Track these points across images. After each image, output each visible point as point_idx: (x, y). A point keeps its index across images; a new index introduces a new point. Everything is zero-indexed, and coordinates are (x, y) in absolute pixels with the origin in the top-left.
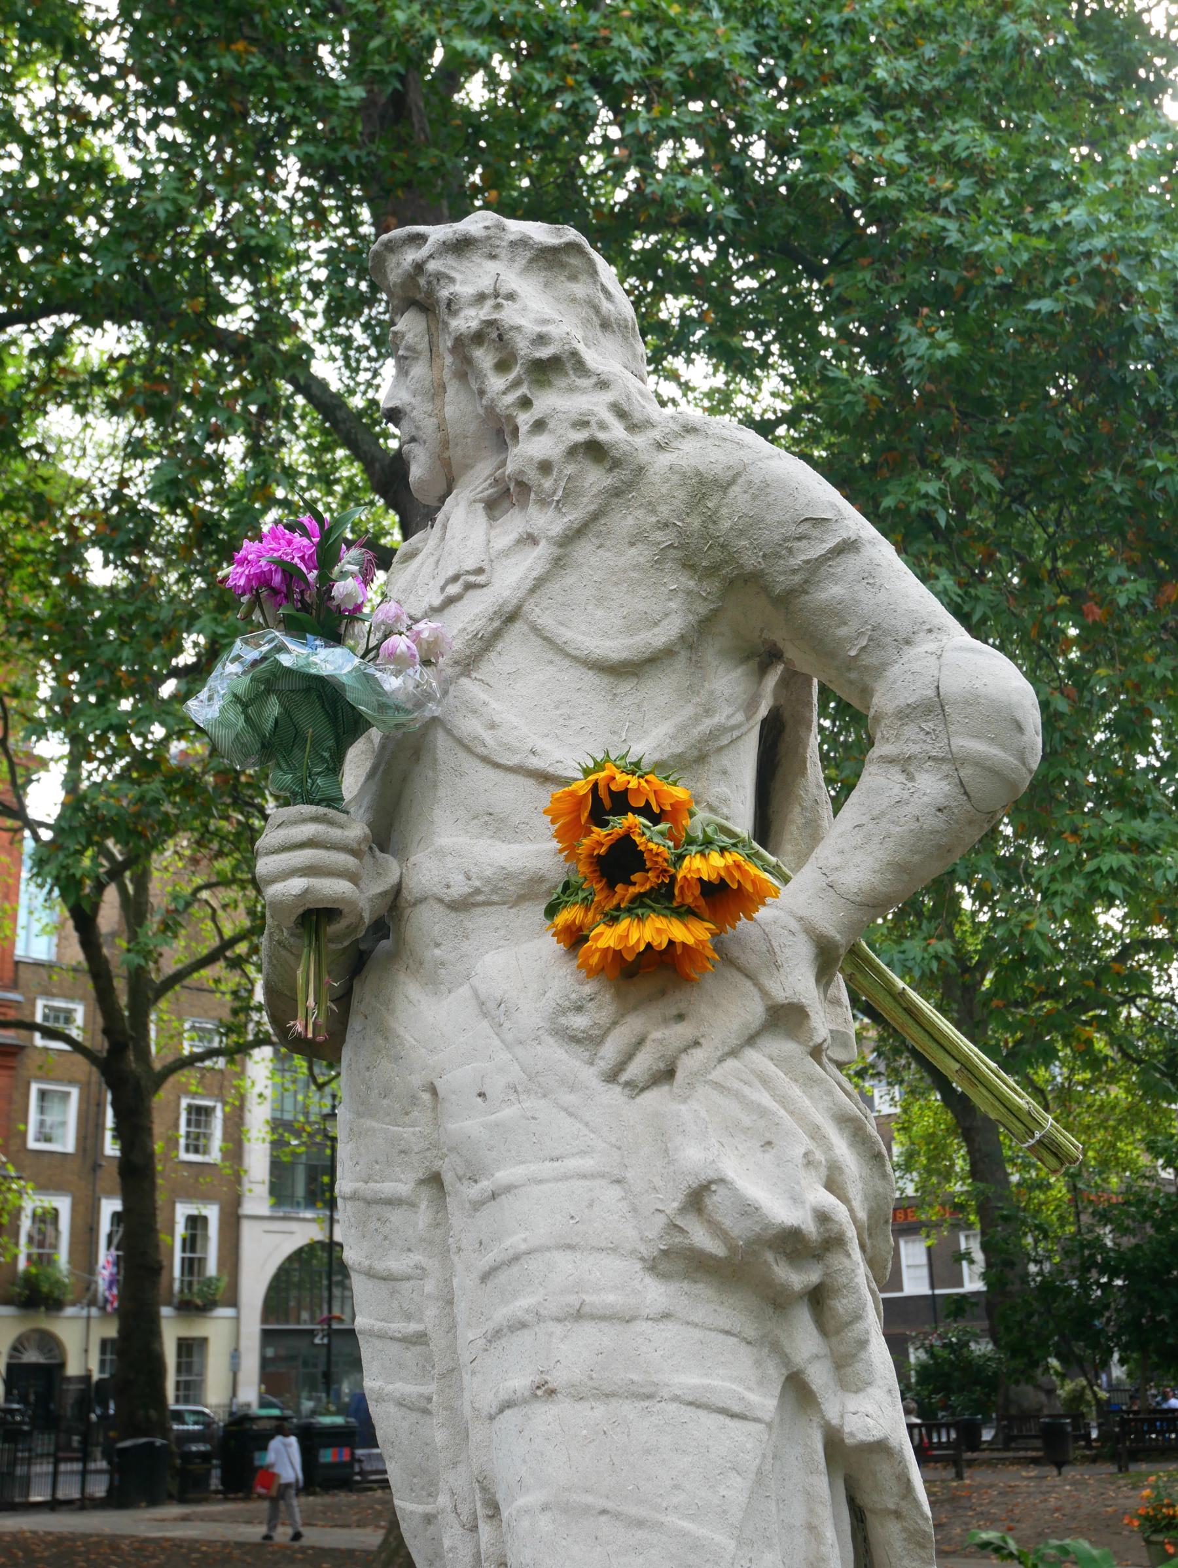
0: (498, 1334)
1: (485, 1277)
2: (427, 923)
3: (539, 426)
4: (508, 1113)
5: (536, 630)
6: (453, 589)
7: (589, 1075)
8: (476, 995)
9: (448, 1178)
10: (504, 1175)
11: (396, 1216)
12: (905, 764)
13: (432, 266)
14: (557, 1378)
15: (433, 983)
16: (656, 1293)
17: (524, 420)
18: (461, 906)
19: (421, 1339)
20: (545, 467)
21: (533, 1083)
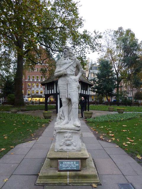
2: (68, 75)
15: (68, 77)
16: (77, 88)
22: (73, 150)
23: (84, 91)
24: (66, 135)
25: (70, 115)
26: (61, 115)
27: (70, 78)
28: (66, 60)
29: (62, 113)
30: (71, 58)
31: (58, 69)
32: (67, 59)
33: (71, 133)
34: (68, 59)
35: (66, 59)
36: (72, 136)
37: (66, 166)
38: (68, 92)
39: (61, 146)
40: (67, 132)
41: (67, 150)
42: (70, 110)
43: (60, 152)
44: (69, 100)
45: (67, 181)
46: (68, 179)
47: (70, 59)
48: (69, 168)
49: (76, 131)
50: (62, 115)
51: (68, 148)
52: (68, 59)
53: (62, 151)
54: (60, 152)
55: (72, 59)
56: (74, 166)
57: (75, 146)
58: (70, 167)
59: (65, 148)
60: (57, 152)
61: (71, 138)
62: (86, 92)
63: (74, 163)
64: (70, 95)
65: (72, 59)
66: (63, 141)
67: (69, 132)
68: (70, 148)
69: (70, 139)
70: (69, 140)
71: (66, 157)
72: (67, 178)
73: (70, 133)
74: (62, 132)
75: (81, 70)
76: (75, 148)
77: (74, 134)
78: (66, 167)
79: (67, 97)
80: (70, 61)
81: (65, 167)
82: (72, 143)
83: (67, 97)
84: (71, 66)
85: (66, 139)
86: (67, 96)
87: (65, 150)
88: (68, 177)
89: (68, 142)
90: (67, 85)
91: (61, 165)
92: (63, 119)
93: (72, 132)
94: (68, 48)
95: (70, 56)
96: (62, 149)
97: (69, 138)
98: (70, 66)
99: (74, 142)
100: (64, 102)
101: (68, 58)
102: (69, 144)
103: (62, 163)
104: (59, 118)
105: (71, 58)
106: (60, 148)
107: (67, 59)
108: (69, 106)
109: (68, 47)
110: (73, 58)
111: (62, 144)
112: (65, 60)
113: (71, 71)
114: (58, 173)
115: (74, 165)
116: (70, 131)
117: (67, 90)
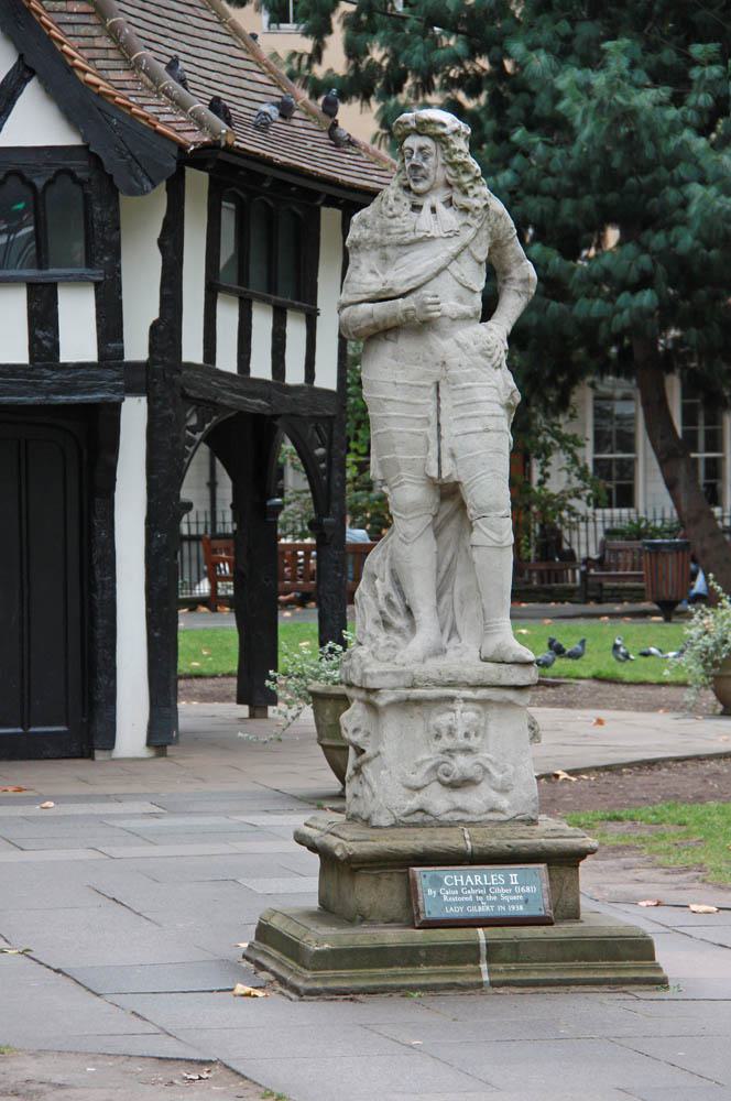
0: (462, 418)
1: (455, 406)
2: (446, 322)
3: (475, 196)
4: (468, 370)
5: (471, 252)
6: (451, 234)
7: (489, 365)
8: (457, 342)
9: (442, 383)
10: (465, 384)
11: (422, 390)
12: (519, 294)
13: (451, 137)
14: (490, 428)
15: (443, 336)
16: (502, 412)
17: (471, 192)
18: (454, 320)
19: (427, 418)
20: (477, 208)
21: (476, 365)
22: (491, 816)
23: (262, 322)
24: (443, 719)
25: (445, 599)
26: (388, 598)
27: (459, 344)
28: (426, 211)
29: (390, 589)
30: (458, 199)
31: (370, 278)
32: (433, 210)
33: (478, 707)
34: (440, 208)
35: (427, 203)
36: (485, 728)
37: (460, 895)
38: (439, 437)
39: (418, 789)
40: (452, 699)
41: (459, 816)
42: (444, 567)
43: (415, 825)
44: (449, 494)
45: (479, 973)
46: (484, 966)
47: (449, 203)
48: (484, 910)
49: (511, 695)
50: (395, 599)
51: (459, 804)
52: (440, 208)
53: (421, 818)
54: (415, 825)
55: (466, 210)
56: (514, 893)
57: (504, 791)
58: (489, 903)
59: (440, 802)
60: (393, 826)
61: (479, 739)
62: (295, 331)
63: (508, 880)
64: (453, 456)
65: (466, 210)
66: (426, 756)
67: (466, 700)
68: (474, 800)
69: (474, 742)
70: (468, 751)
71: (462, 845)
72: (476, 961)
73: (470, 706)
74: (418, 702)
75: (516, 274)
76: (504, 802)
77: (494, 712)
78: (470, 903)
79: (434, 474)
80: (450, 218)
81: (458, 904)
82: (486, 771)
83: (434, 474)
84: (464, 257)
85: (447, 742)
86: (433, 464)
87: (447, 817)
88: (484, 951)
89: (462, 765)
90: (432, 391)
91: (430, 892)
92: (399, 631)
93: (485, 702)
94: (441, 130)
95: (448, 185)
96: (421, 810)
97: (467, 735)
98: (456, 257)
99: (495, 764)
100: (415, 506)
101: (436, 199)
102: (470, 773)
103: (437, 883)
104: (377, 622)
105: (458, 199)
106: (413, 803)
107: (433, 210)
108: (438, 532)
109: (444, 125)
110: (477, 202)
111: (418, 778)
112: (416, 208)
113: (466, 294)
114: (419, 936)
115: (517, 891)
116: (468, 693)
117: (434, 423)
